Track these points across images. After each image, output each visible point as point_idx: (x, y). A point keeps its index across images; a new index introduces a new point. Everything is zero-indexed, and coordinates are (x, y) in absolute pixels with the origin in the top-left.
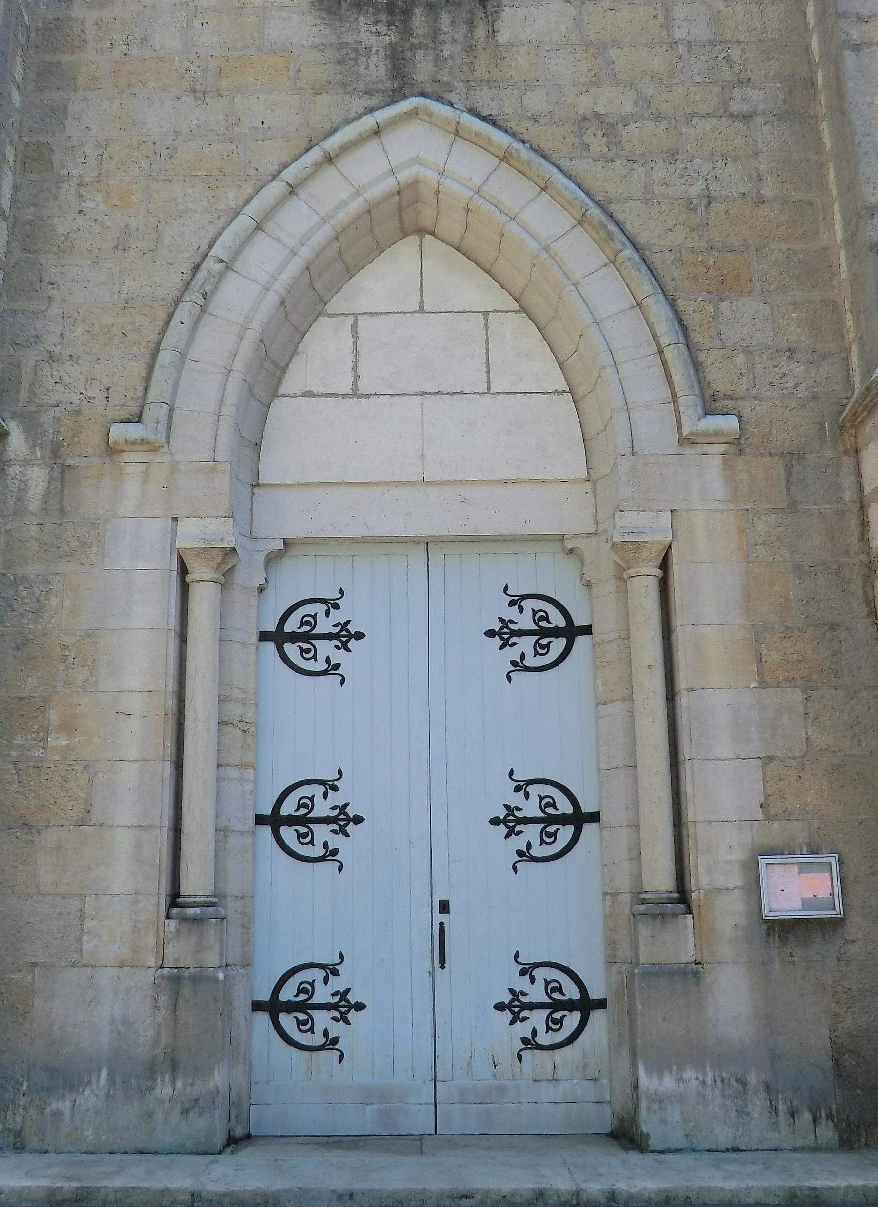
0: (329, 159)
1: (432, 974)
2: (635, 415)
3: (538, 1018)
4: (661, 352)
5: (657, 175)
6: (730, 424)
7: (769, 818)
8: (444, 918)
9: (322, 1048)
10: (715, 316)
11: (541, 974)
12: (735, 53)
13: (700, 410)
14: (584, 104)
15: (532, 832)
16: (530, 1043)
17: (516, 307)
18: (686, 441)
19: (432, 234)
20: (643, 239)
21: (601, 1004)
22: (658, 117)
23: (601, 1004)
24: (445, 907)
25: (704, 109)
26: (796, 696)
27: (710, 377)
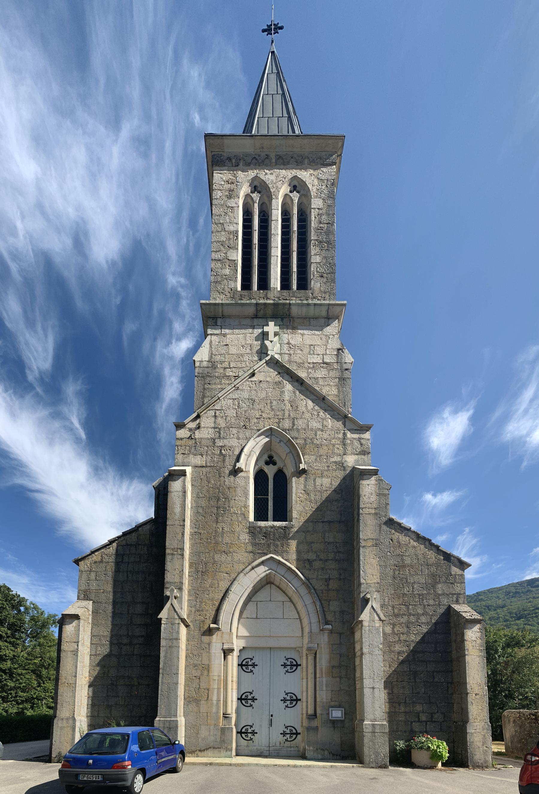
0: (253, 568)
1: (269, 728)
2: (312, 625)
3: (288, 736)
4: (317, 612)
5: (319, 573)
6: (329, 627)
7: (332, 701)
8: (272, 718)
9: (250, 740)
10: (329, 605)
11: (289, 728)
12: (338, 545)
13: (324, 624)
14: (306, 557)
15: (288, 702)
16: (286, 740)
17: (289, 600)
18: (321, 630)
19: (273, 584)
20: (315, 588)
21: (300, 734)
22: (321, 560)
23: (300, 734)
24: (272, 716)
25: (330, 558)
26: (338, 679)
27: (327, 617)
